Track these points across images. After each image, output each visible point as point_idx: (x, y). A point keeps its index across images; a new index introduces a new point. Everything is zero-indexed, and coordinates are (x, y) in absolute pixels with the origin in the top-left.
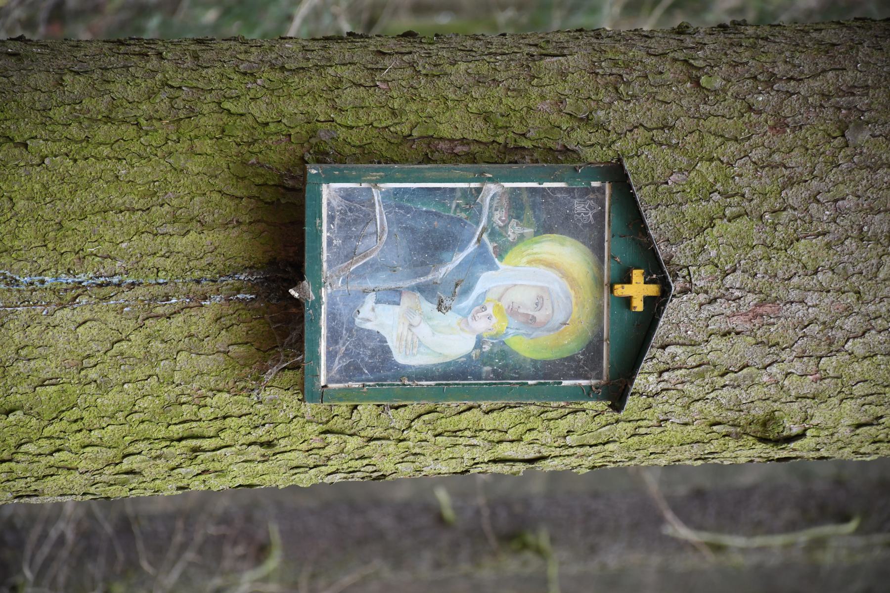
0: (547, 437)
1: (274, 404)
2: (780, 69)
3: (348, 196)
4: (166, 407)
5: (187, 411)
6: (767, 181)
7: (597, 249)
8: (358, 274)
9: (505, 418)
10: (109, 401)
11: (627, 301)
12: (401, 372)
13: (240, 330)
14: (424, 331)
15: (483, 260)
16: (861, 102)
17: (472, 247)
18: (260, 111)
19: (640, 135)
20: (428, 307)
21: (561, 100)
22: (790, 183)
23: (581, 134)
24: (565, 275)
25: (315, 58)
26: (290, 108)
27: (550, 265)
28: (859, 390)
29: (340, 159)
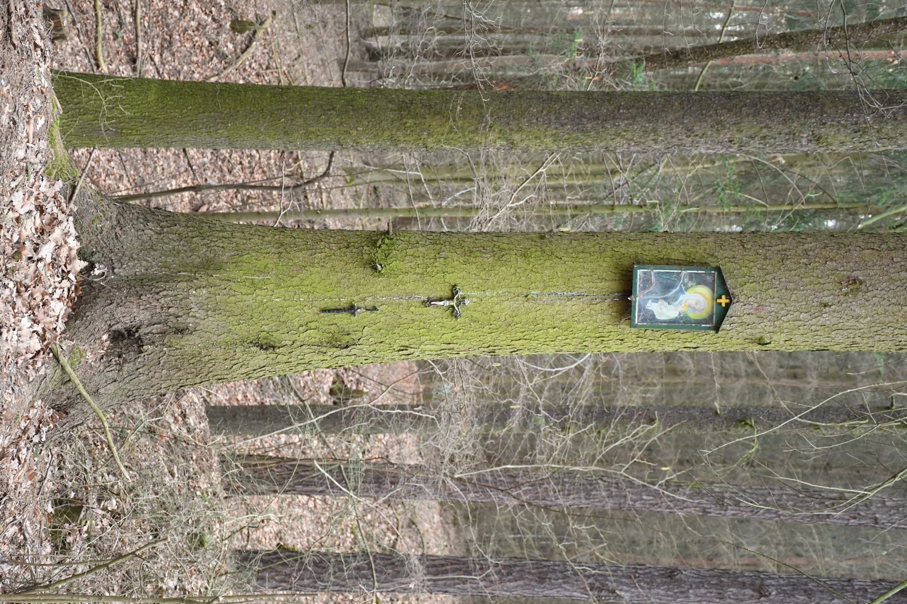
0: (699, 341)
1: (624, 329)
2: (767, 243)
3: (645, 273)
4: (595, 329)
5: (600, 330)
6: (761, 273)
7: (713, 290)
8: (647, 294)
9: (687, 335)
10: (580, 326)
11: (720, 304)
12: (658, 321)
13: (615, 309)
14: (664, 310)
15: (681, 291)
16: (788, 253)
17: (678, 288)
18: (623, 251)
19: (727, 260)
20: (666, 304)
21: (705, 250)
22: (768, 274)
23: (710, 259)
24: (704, 296)
25: (639, 237)
26: (631, 250)
27: (700, 294)
28: (785, 331)
29: (644, 263)
